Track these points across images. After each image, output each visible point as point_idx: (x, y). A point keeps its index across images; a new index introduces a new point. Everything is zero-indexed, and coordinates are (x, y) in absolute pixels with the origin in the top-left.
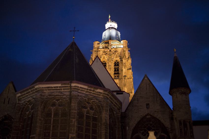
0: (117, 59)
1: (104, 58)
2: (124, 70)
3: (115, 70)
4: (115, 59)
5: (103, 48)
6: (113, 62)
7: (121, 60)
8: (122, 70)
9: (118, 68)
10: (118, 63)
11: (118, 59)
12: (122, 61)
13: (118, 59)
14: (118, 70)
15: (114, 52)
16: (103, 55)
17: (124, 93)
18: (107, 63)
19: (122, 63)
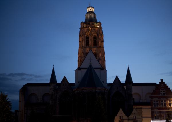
0: (95, 35)
1: (87, 34)
2: (100, 42)
3: (94, 42)
4: (94, 35)
5: (87, 27)
6: (93, 37)
7: (98, 36)
8: (98, 42)
9: (96, 40)
10: (96, 37)
11: (96, 35)
12: (98, 36)
13: (96, 35)
14: (96, 42)
15: (93, 30)
16: (87, 32)
17: (104, 69)
18: (89, 37)
19: (98, 37)
